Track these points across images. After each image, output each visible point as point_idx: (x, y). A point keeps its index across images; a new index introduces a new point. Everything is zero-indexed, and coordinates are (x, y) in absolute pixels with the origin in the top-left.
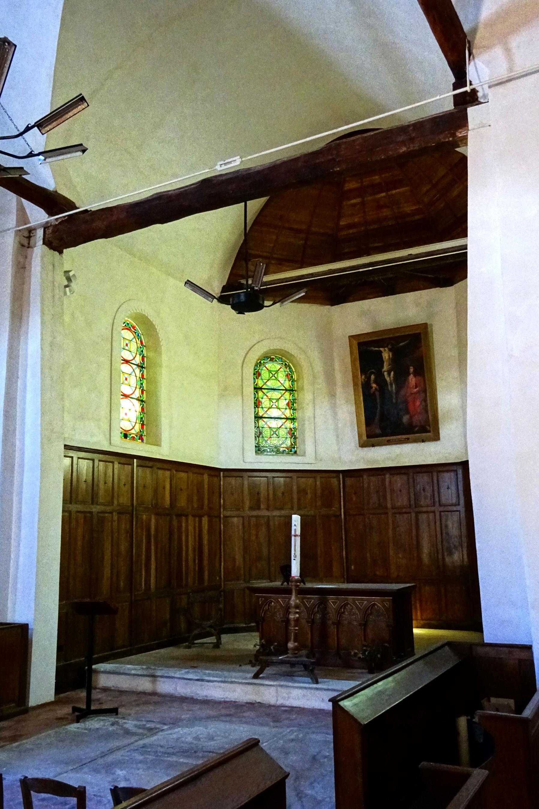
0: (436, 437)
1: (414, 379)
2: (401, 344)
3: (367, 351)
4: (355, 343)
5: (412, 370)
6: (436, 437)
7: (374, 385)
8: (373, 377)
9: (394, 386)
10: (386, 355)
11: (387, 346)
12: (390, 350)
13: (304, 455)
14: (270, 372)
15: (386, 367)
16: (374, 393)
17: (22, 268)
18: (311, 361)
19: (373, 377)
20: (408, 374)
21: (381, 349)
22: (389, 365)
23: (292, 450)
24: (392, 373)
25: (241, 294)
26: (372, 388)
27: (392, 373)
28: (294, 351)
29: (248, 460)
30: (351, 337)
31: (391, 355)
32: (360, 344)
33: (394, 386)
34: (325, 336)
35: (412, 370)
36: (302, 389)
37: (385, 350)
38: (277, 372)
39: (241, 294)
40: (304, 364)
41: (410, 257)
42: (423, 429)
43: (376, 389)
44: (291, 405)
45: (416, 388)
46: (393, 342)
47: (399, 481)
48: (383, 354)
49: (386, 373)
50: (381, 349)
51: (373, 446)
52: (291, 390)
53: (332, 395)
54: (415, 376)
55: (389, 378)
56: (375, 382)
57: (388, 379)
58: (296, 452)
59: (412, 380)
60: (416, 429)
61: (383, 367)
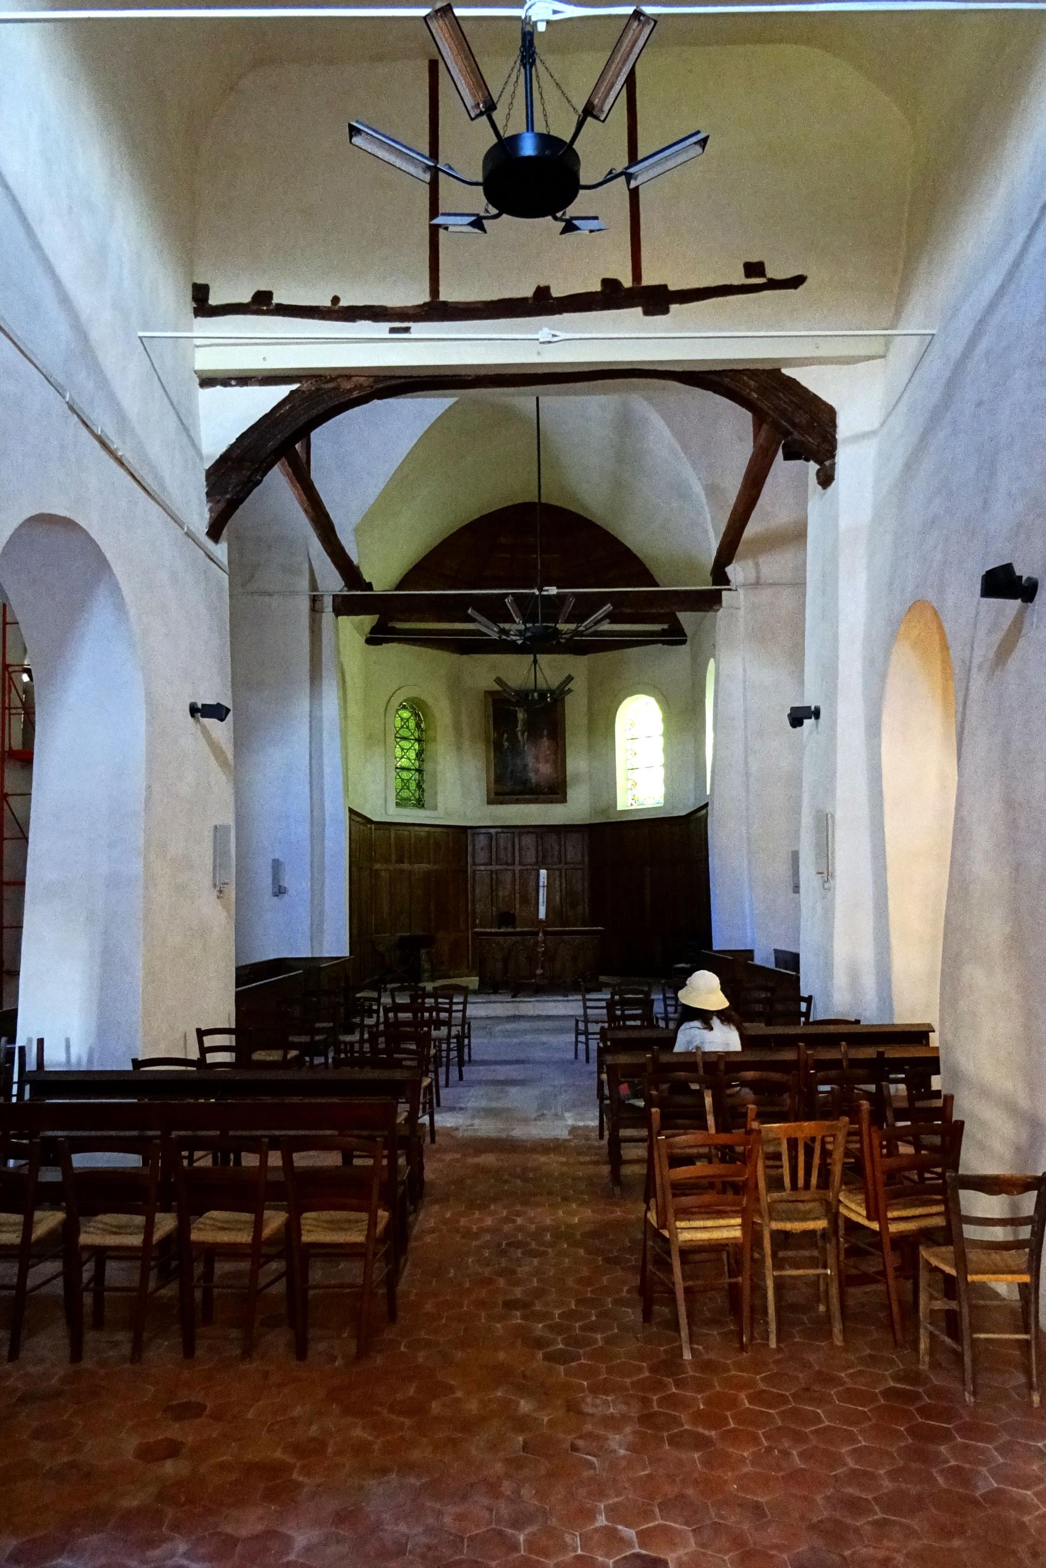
0: (564, 800)
4: (490, 700)
5: (545, 733)
6: (564, 800)
7: (506, 744)
10: (521, 715)
13: (435, 808)
14: (402, 719)
18: (442, 712)
20: (542, 737)
23: (420, 804)
28: (430, 701)
32: (494, 701)
34: (455, 687)
35: (545, 733)
36: (435, 740)
40: (438, 715)
44: (419, 755)
49: (519, 734)
51: (502, 803)
52: (419, 740)
53: (459, 748)
57: (520, 738)
58: (423, 806)
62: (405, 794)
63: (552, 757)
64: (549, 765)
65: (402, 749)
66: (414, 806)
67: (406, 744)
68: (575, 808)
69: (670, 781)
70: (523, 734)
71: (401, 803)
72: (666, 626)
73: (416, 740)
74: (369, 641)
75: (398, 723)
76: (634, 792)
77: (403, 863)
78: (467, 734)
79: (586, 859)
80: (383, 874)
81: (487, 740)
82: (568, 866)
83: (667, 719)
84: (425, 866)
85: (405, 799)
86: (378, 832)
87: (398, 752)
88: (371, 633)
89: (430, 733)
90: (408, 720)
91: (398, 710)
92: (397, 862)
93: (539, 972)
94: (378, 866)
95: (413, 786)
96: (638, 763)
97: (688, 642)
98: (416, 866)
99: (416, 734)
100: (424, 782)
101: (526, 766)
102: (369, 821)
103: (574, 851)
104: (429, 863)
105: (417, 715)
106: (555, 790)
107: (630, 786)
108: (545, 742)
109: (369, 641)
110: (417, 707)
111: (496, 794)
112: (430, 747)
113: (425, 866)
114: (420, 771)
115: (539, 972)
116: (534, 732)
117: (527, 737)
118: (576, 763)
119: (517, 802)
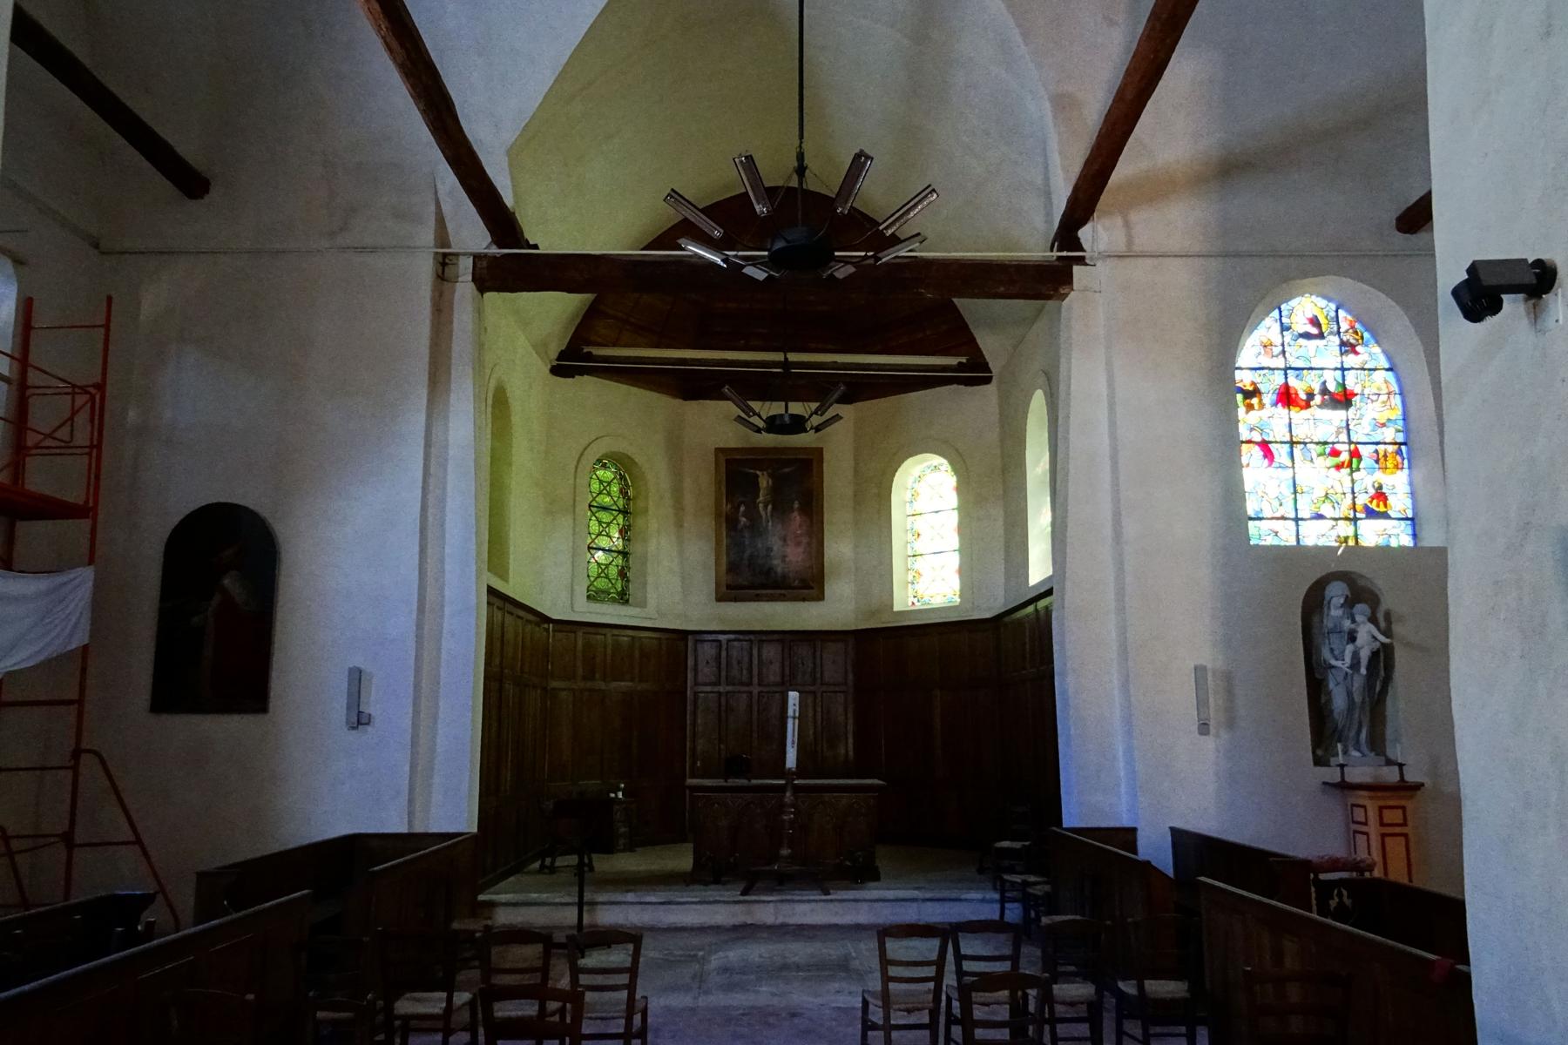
3: (736, 473)
5: (796, 505)
10: (764, 482)
12: (770, 475)
14: (601, 482)
17: (441, 309)
19: (742, 508)
20: (792, 510)
23: (623, 598)
25: (571, 361)
30: (718, 450)
35: (796, 505)
36: (646, 510)
39: (571, 361)
41: (835, 365)
42: (805, 585)
51: (736, 600)
52: (625, 512)
53: (679, 525)
55: (765, 511)
58: (627, 601)
62: (601, 584)
63: (805, 540)
64: (800, 550)
65: (600, 523)
66: (613, 600)
67: (605, 517)
68: (836, 609)
69: (969, 571)
70: (766, 507)
71: (594, 596)
72: (964, 360)
73: (620, 511)
74: (557, 371)
75: (595, 486)
76: (917, 587)
77: (593, 678)
78: (689, 500)
79: (851, 677)
80: (563, 695)
81: (718, 515)
82: (824, 688)
83: (960, 489)
84: (624, 685)
85: (603, 592)
86: (559, 635)
87: (594, 527)
89: (640, 504)
90: (609, 484)
91: (595, 470)
92: (584, 678)
93: (785, 852)
94: (555, 684)
95: (613, 571)
96: (924, 546)
97: (994, 380)
98: (614, 685)
99: (621, 503)
101: (770, 549)
102: (548, 620)
103: (834, 665)
104: (632, 680)
105: (622, 477)
106: (810, 585)
107: (910, 578)
108: (796, 518)
109: (557, 371)
110: (623, 465)
111: (728, 587)
112: (639, 522)
113: (624, 685)
114: (624, 554)
115: (785, 852)
116: (780, 508)
117: (774, 507)
118: (839, 548)
119: (757, 598)
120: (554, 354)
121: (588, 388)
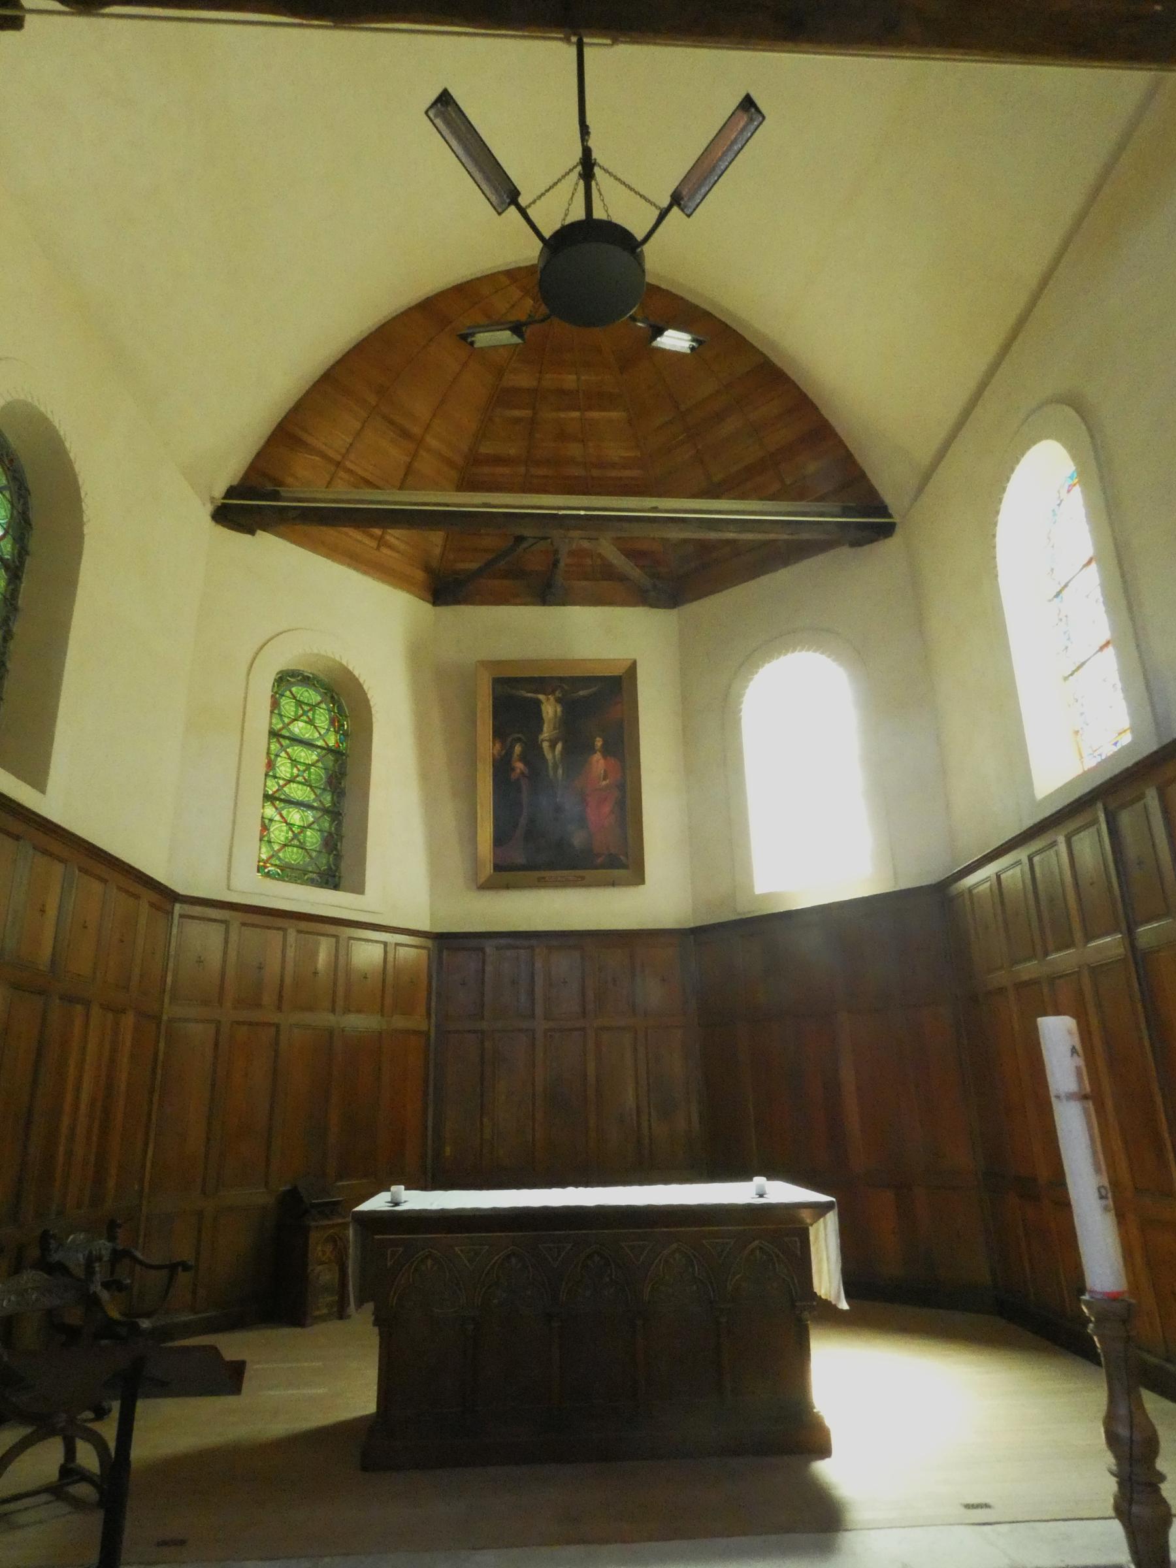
1: (602, 761)
2: (581, 693)
5: (599, 742)
7: (519, 766)
8: (518, 749)
9: (560, 771)
10: (550, 710)
11: (553, 693)
12: (558, 700)
15: (547, 732)
16: (518, 779)
19: (518, 749)
20: (591, 749)
21: (541, 697)
22: (555, 728)
23: (331, 879)
24: (559, 746)
26: (513, 769)
27: (559, 746)
29: (236, 883)
31: (559, 709)
33: (560, 771)
35: (599, 742)
37: (548, 699)
38: (313, 707)
42: (614, 862)
43: (522, 773)
45: (604, 779)
46: (566, 687)
47: (563, 964)
48: (543, 708)
49: (545, 745)
50: (541, 697)
54: (605, 757)
55: (552, 754)
56: (523, 758)
57: (549, 756)
59: (598, 763)
60: (599, 861)
61: (540, 730)
70: (553, 746)
74: (225, 515)
88: (224, 498)
95: (312, 838)
100: (341, 837)
101: (558, 809)
111: (497, 868)
119: (542, 884)
120: (219, 490)
121: (271, 550)
